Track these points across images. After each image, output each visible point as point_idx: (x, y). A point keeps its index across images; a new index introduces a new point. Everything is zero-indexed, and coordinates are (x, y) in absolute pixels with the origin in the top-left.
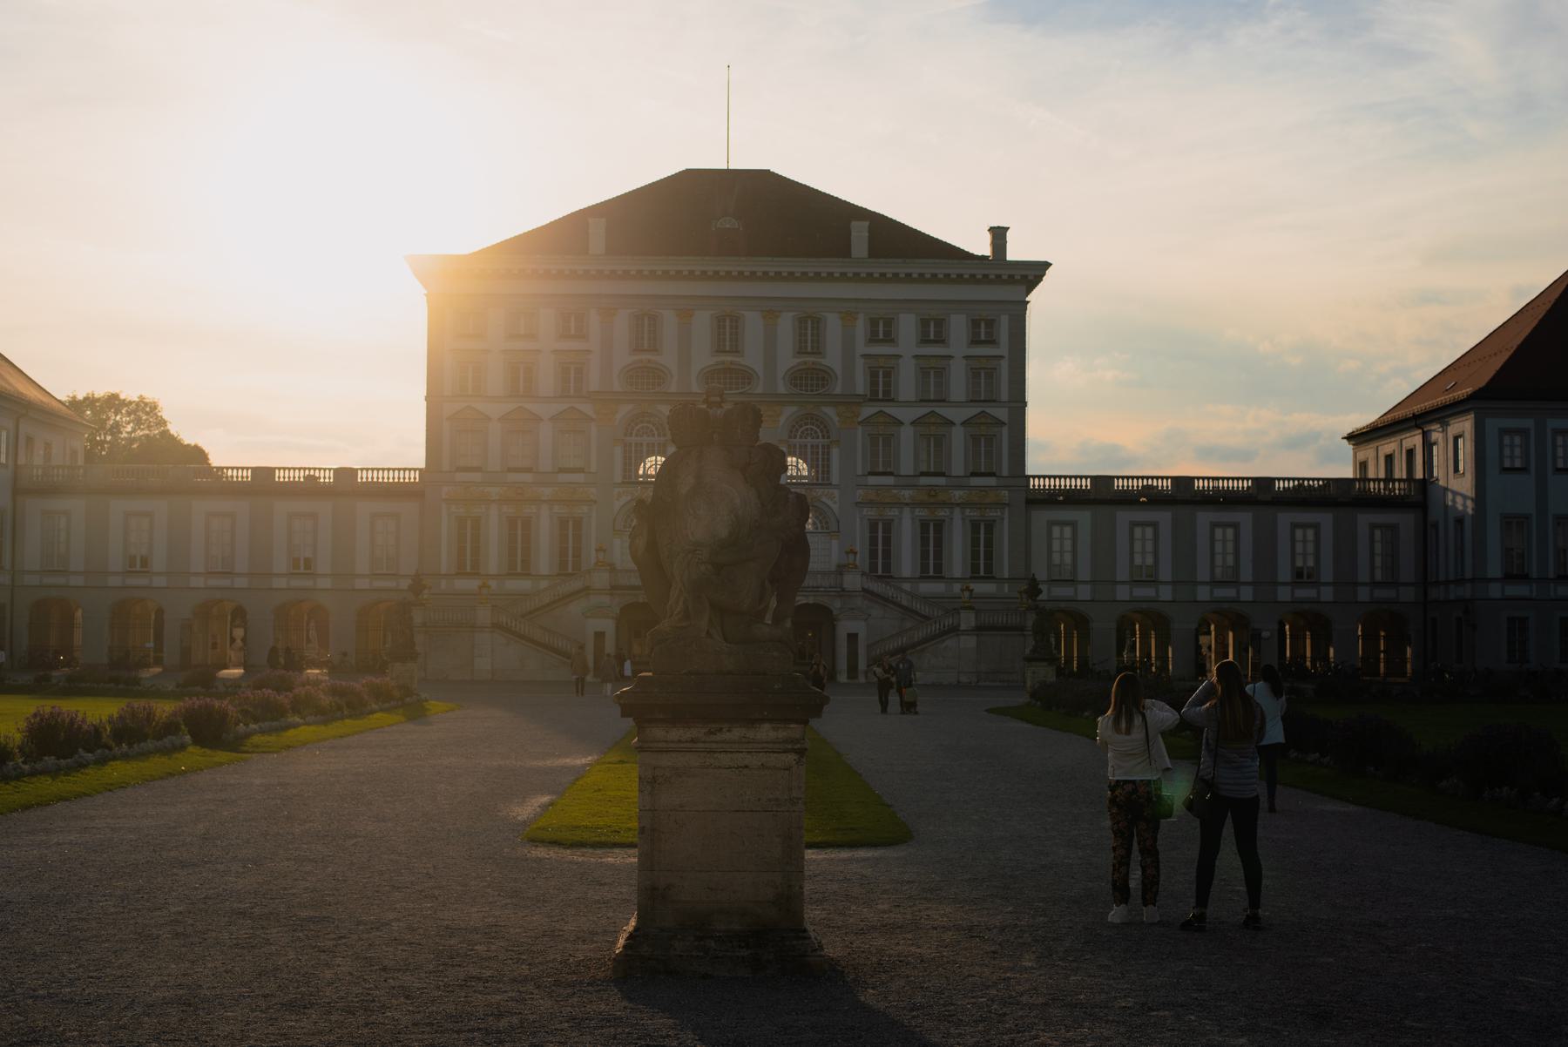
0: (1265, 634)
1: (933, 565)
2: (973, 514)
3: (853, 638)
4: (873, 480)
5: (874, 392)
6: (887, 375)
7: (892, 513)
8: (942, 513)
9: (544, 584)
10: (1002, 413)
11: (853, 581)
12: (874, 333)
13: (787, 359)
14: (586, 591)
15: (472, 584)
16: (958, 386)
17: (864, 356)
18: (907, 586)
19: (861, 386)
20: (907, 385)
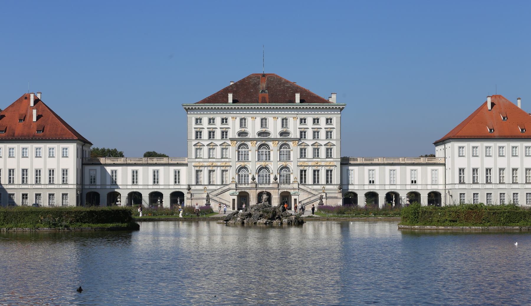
0: (403, 198)
1: (316, 181)
2: (328, 168)
3: (295, 200)
4: (301, 160)
5: (301, 137)
6: (305, 132)
7: (306, 168)
8: (319, 168)
9: (219, 187)
10: (334, 142)
11: (296, 186)
12: (301, 122)
13: (280, 129)
14: (229, 189)
15: (201, 187)
16: (322, 134)
17: (299, 128)
18: (310, 187)
19: (298, 137)
20: (309, 135)
